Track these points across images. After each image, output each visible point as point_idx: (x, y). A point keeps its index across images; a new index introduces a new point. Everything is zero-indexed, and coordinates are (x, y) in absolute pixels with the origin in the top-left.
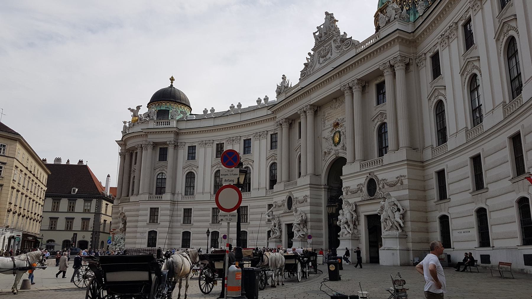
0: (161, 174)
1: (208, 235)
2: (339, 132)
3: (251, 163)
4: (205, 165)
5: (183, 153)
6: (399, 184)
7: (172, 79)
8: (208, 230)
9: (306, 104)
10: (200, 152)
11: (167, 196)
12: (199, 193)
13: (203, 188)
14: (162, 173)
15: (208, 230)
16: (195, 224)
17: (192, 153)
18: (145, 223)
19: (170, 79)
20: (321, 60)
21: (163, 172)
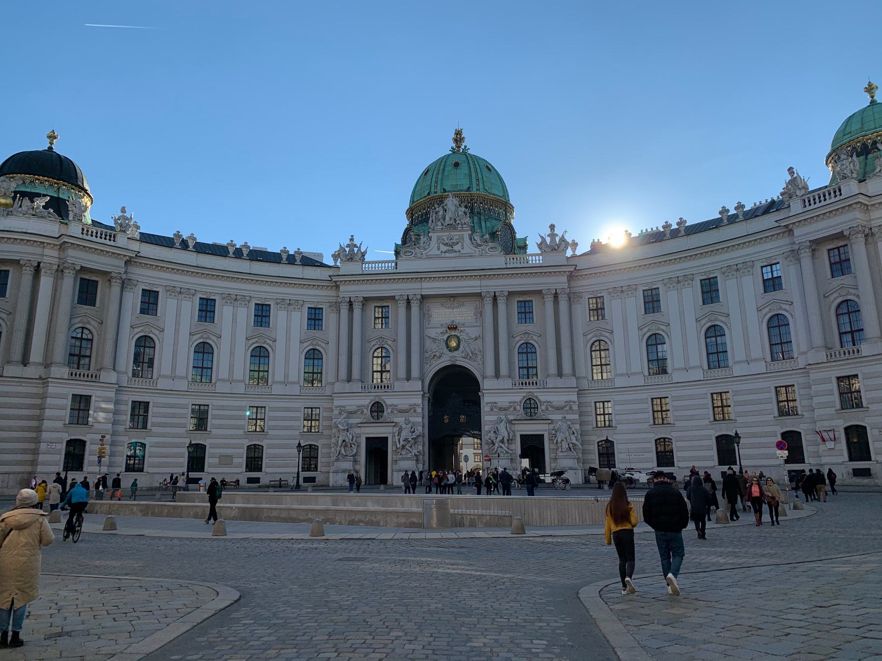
0: (80, 330)
1: (299, 451)
2: (458, 337)
3: (271, 343)
4: (177, 331)
5: (133, 300)
6: (567, 408)
7: (52, 137)
8: (299, 444)
9: (418, 292)
10: (167, 305)
11: (110, 377)
12: (165, 377)
13: (174, 369)
14: (83, 328)
15: (299, 444)
16: (154, 429)
17: (150, 301)
18: (59, 424)
19: (49, 137)
20: (444, 248)
21: (88, 326)
